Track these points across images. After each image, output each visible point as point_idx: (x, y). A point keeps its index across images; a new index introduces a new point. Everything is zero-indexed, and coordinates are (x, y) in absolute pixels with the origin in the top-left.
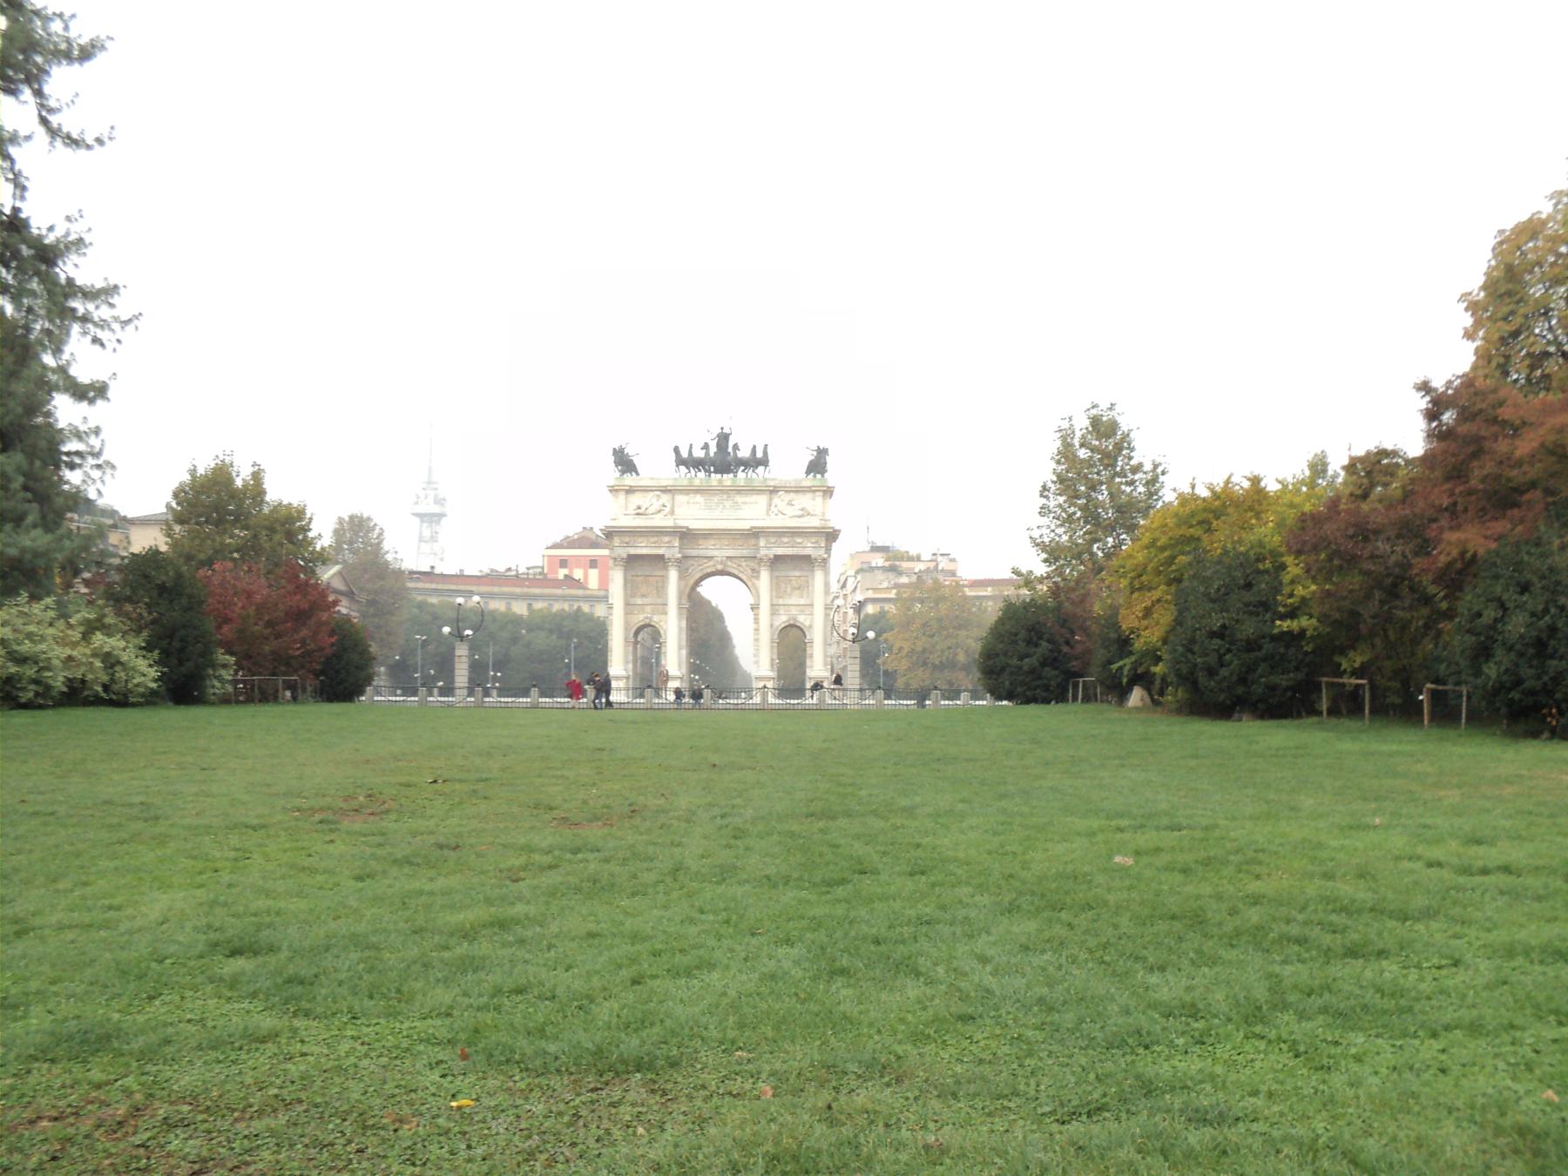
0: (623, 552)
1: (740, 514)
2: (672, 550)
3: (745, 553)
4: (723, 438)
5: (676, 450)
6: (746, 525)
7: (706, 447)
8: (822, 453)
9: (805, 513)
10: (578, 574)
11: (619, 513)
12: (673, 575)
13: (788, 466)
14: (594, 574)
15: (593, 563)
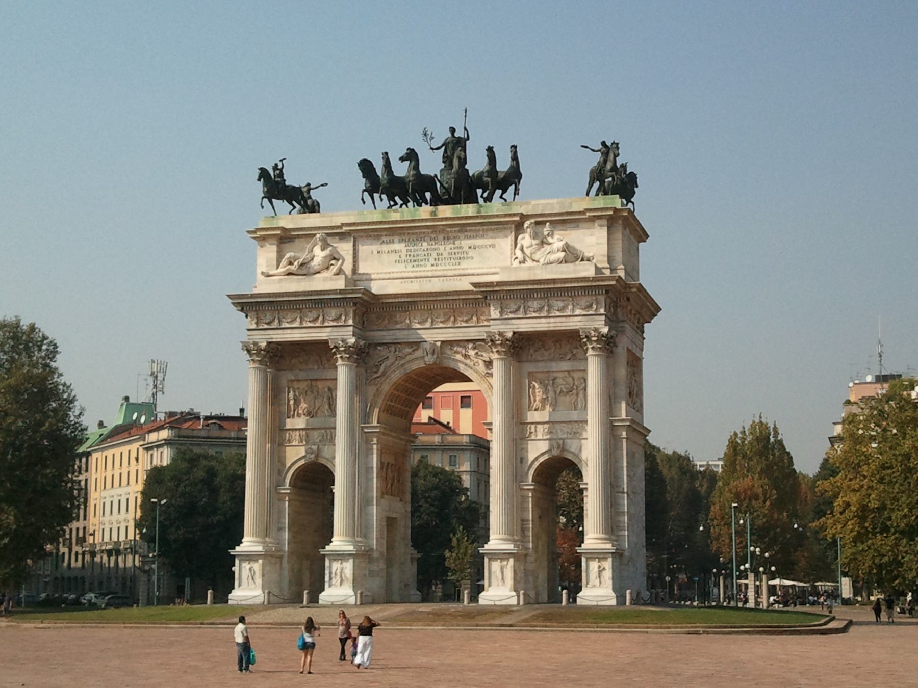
0: (262, 339)
1: (467, 266)
2: (341, 332)
3: (473, 333)
4: (455, 147)
5: (366, 167)
6: (464, 285)
7: (411, 156)
8: (608, 150)
9: (572, 255)
10: (446, 416)
11: (267, 275)
12: (343, 374)
13: (556, 182)
14: (466, 415)
15: (465, 401)
